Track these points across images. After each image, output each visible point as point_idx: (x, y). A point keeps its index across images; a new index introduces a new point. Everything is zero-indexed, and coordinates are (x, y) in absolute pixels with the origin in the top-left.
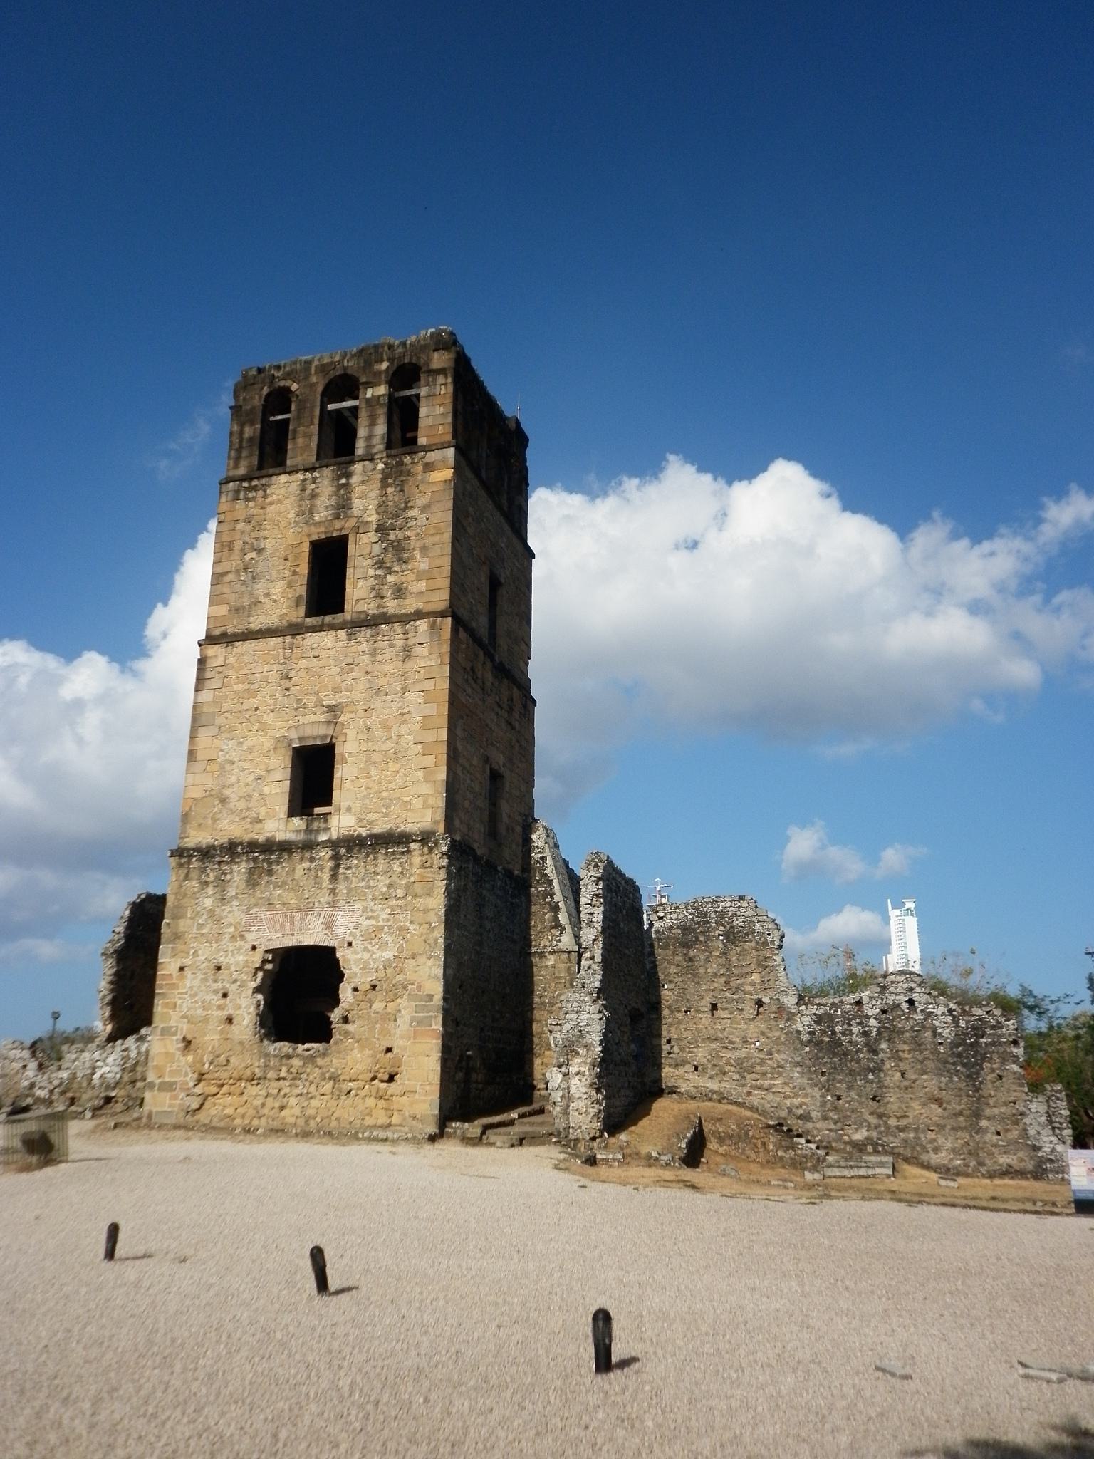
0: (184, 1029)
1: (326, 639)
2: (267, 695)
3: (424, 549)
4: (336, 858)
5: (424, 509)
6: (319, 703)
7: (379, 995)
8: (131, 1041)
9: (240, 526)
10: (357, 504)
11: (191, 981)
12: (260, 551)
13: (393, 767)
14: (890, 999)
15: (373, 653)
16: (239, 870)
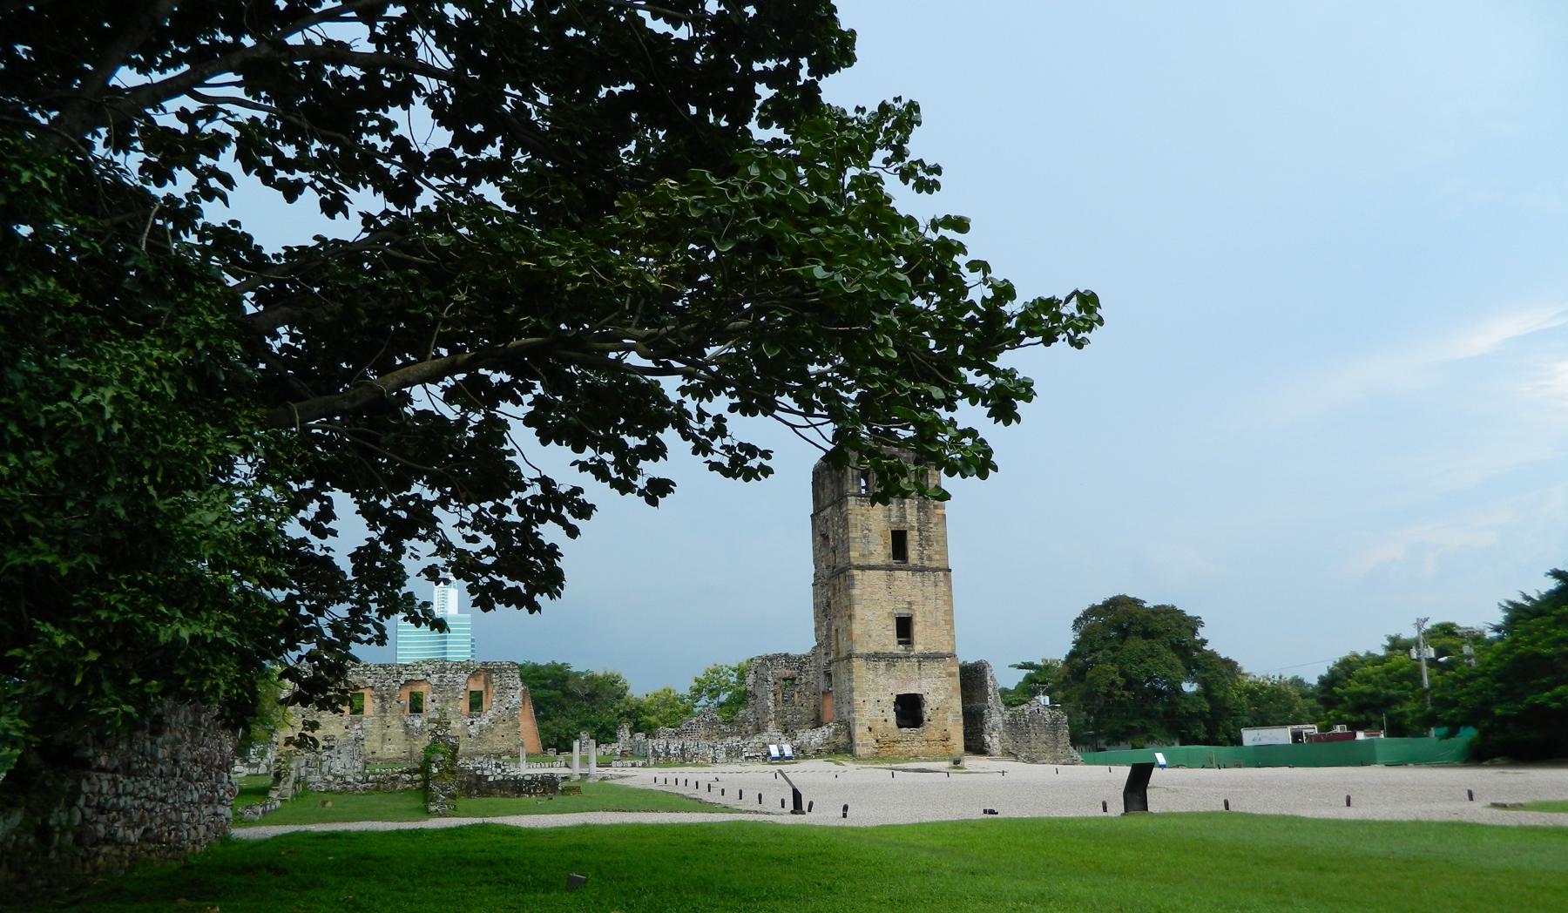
0: (868, 724)
1: (902, 574)
2: (882, 594)
3: (937, 542)
4: (918, 661)
5: (936, 524)
6: (903, 600)
7: (940, 711)
8: (824, 728)
9: (859, 517)
10: (908, 516)
11: (868, 706)
12: (870, 531)
13: (935, 628)
14: (1032, 708)
15: (923, 582)
16: (882, 664)
